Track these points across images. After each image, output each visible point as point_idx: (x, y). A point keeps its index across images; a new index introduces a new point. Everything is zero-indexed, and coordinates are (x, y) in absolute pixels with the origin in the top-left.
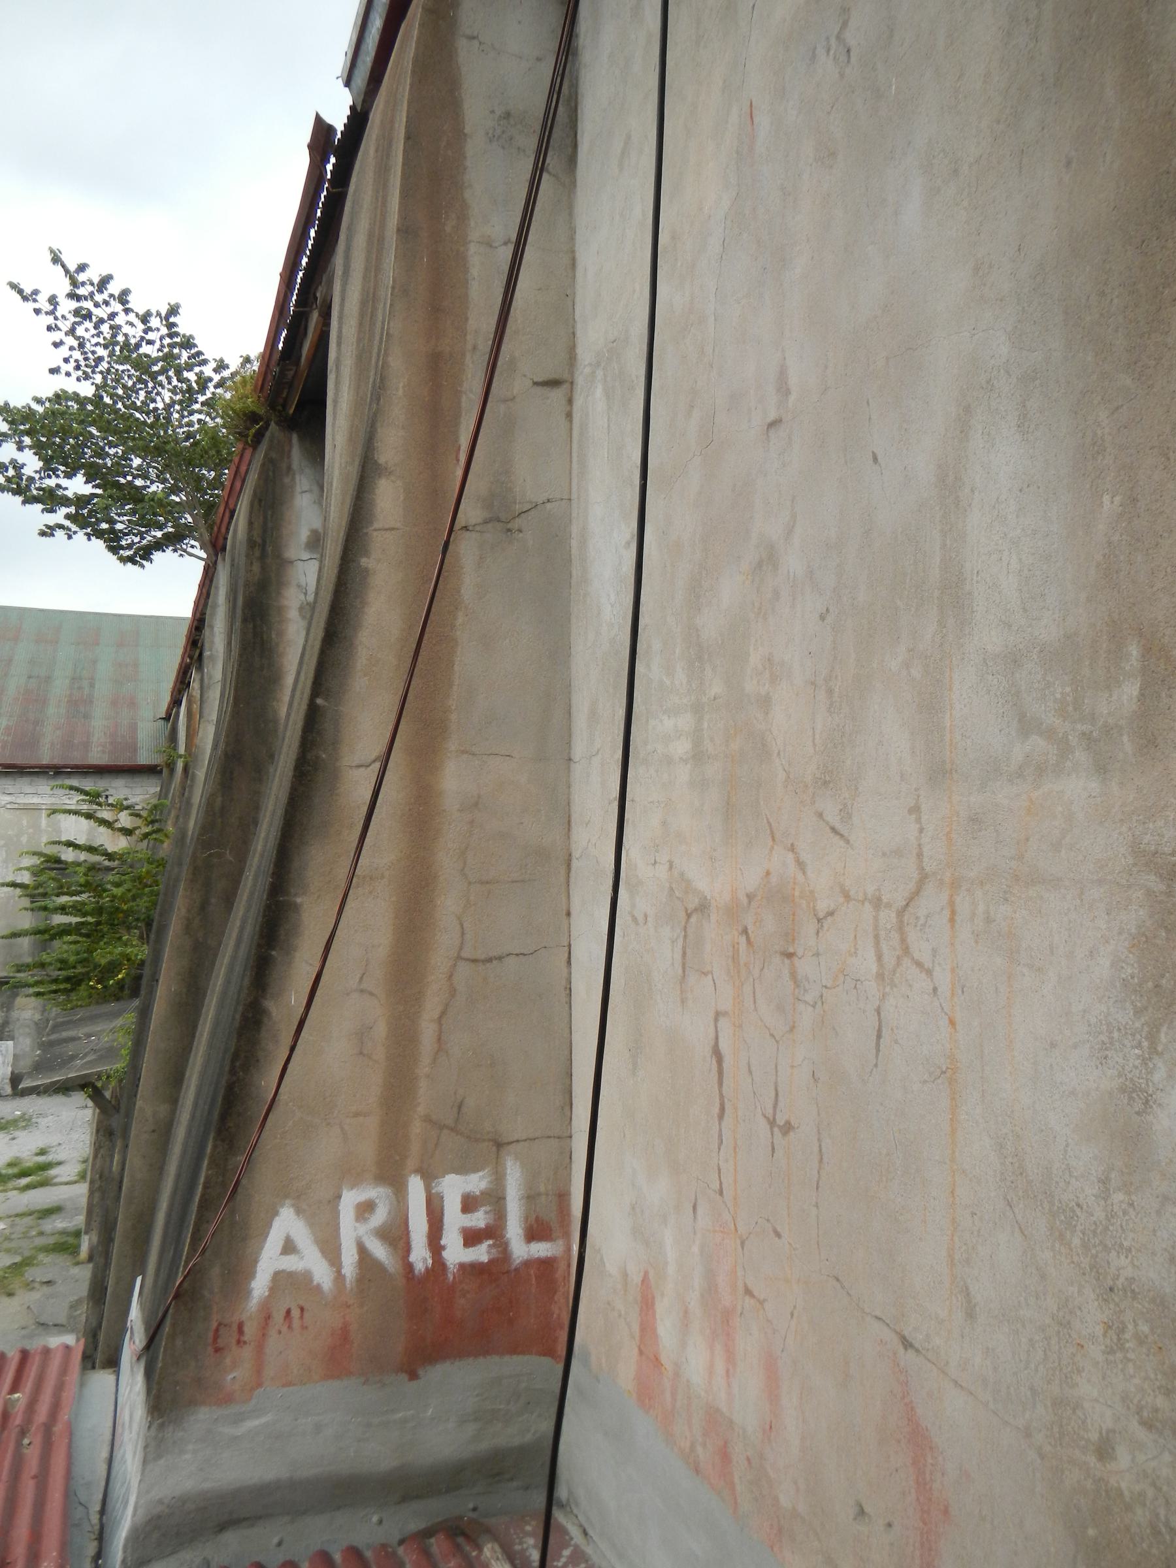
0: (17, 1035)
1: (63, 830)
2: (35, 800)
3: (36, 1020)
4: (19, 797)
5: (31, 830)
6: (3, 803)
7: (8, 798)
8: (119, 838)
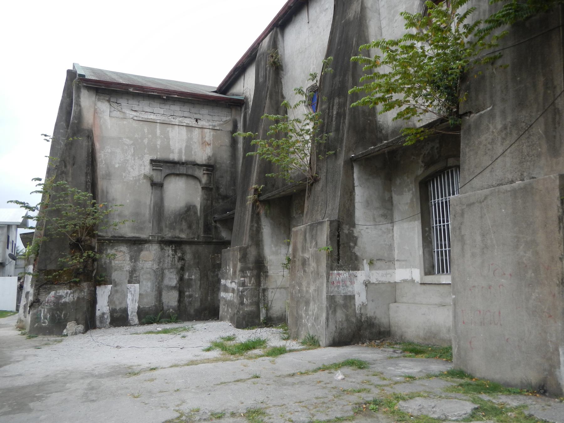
0: (141, 280)
1: (171, 137)
2: (152, 117)
3: (154, 269)
4: (142, 114)
5: (150, 136)
6: (131, 116)
7: (135, 114)
8: (206, 147)
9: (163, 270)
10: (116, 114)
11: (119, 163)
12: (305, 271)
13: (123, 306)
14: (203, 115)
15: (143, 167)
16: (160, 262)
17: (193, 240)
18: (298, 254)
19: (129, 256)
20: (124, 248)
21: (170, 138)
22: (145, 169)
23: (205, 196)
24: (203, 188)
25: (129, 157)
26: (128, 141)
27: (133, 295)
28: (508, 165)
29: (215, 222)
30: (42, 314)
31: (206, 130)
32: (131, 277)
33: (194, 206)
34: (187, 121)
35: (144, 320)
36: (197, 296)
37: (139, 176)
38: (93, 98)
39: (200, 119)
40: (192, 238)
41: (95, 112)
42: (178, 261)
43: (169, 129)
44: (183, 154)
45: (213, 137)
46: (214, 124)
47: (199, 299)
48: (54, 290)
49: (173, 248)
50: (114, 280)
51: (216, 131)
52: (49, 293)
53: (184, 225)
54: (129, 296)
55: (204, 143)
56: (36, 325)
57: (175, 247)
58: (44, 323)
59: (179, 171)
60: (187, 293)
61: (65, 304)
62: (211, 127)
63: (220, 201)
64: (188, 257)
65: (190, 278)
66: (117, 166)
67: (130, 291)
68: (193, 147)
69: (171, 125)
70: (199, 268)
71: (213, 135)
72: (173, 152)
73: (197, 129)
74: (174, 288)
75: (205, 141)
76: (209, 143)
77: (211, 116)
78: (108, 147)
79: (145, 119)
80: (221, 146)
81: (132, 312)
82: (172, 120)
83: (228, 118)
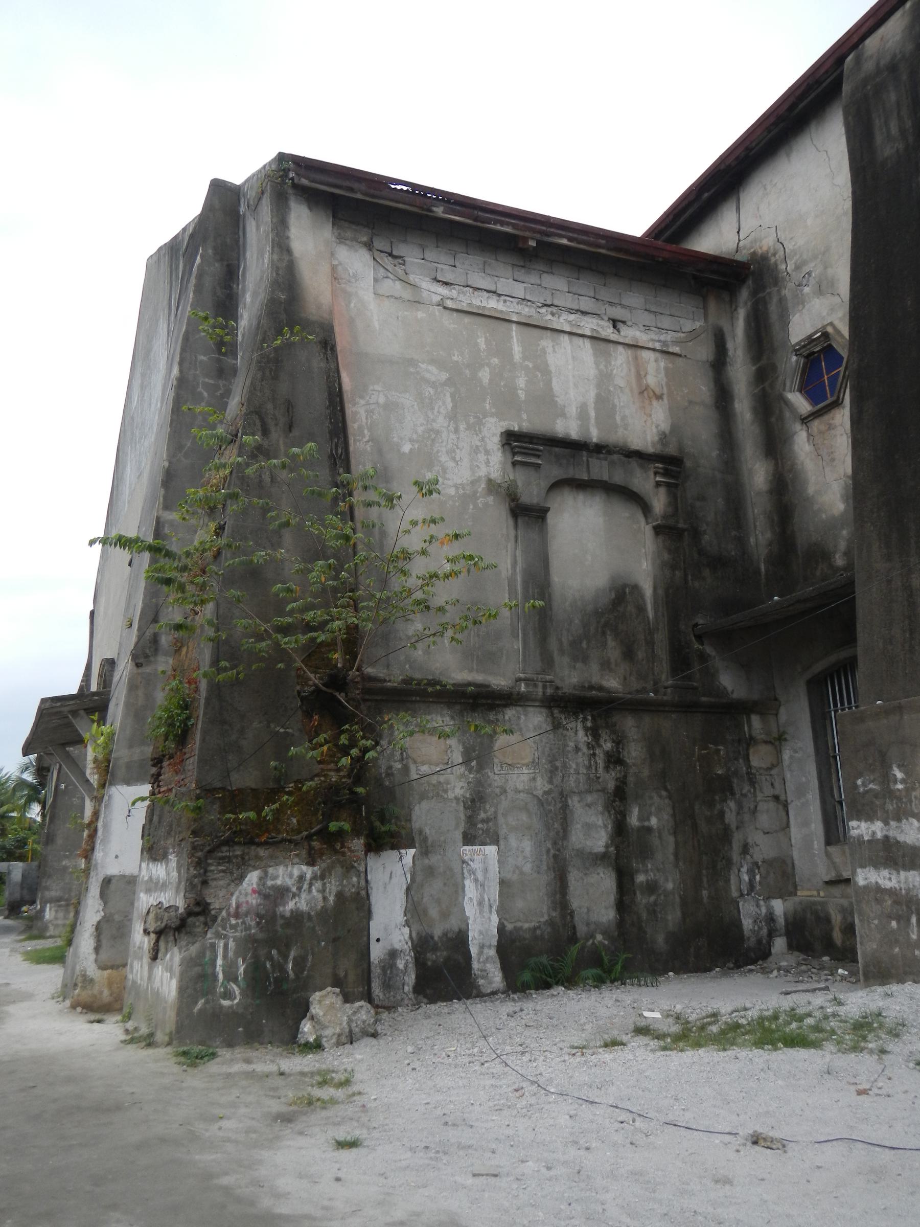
0: (503, 831)
1: (552, 368)
2: (492, 304)
3: (539, 793)
5: (495, 361)
8: (651, 404)
9: (563, 796)
10: (392, 287)
11: (411, 440)
13: (453, 924)
14: (631, 308)
15: (482, 457)
16: (553, 771)
17: (640, 696)
19: (461, 748)
20: (441, 719)
21: (551, 372)
22: (487, 463)
23: (666, 556)
24: (658, 530)
25: (441, 422)
26: (433, 369)
27: (481, 885)
29: (699, 638)
30: (219, 962)
31: (646, 354)
32: (471, 820)
33: (636, 588)
34: (588, 325)
35: (527, 976)
36: (670, 886)
37: (473, 483)
38: (327, 232)
39: (624, 322)
40: (638, 691)
41: (335, 276)
42: (607, 768)
43: (546, 342)
44: (593, 421)
45: (667, 375)
46: (662, 338)
47: (677, 899)
48: (255, 868)
49: (589, 724)
50: (421, 832)
51: (672, 357)
52: (241, 878)
53: (613, 650)
54: (471, 890)
55: (645, 393)
56: (201, 1003)
57: (593, 718)
58: (228, 995)
59: (588, 471)
60: (641, 878)
61: (298, 917)
62: (658, 346)
63: (707, 572)
64: (634, 752)
65: (646, 824)
66: (406, 448)
67: (473, 872)
68: (616, 401)
69: (549, 333)
70: (666, 789)
71: (666, 369)
72: (563, 415)
73: (620, 349)
74: (602, 858)
75: (647, 387)
76: (658, 391)
77: (652, 316)
78: (377, 387)
79: (479, 307)
80: (690, 402)
81: (482, 947)
82: (549, 317)
83: (698, 324)
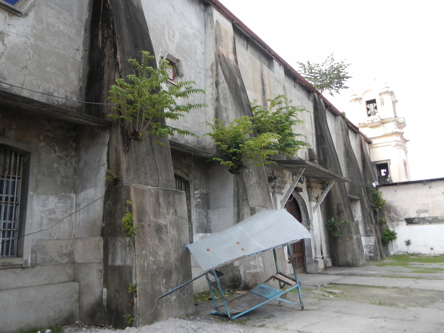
12: (161, 239)
18: (147, 218)
28: (261, 199)
